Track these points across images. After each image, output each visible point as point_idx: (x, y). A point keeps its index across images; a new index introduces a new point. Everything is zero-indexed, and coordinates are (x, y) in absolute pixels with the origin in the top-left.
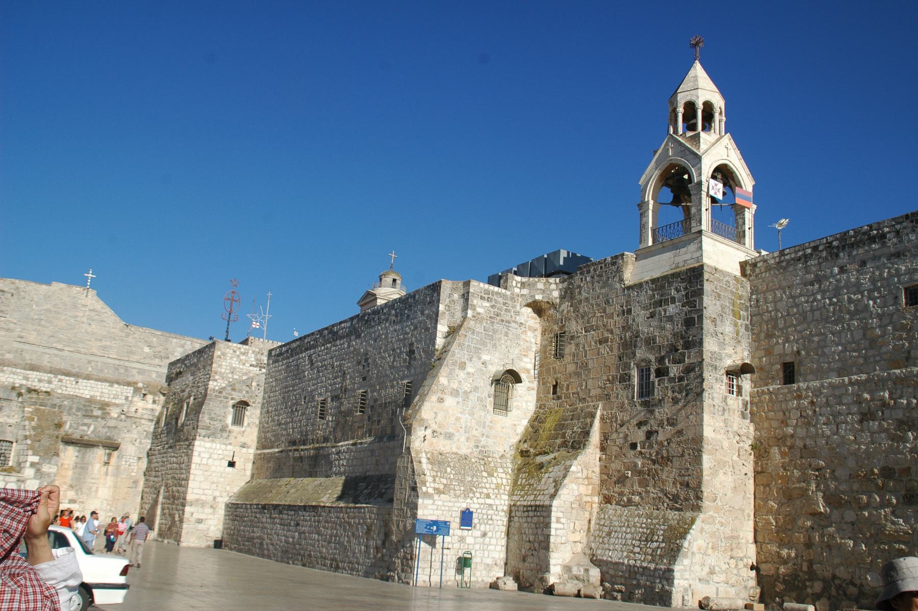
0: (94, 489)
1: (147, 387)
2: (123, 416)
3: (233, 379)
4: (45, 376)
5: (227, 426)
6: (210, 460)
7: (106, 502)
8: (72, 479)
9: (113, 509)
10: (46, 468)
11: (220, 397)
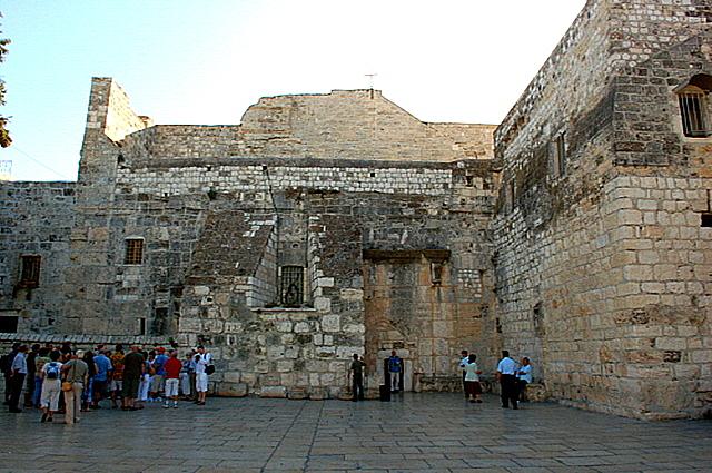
0: (425, 323)
1: (471, 167)
2: (446, 213)
3: (660, 44)
4: (329, 172)
5: (677, 139)
6: (662, 216)
8: (392, 312)
10: (346, 295)
11: (645, 81)
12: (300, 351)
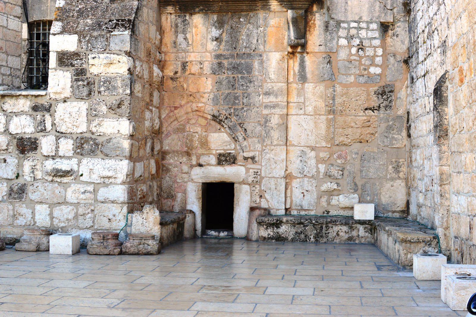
0: (275, 120)
7: (313, 154)
8: (216, 101)
9: (334, 172)
12: (20, 166)
